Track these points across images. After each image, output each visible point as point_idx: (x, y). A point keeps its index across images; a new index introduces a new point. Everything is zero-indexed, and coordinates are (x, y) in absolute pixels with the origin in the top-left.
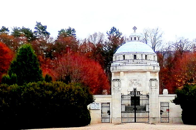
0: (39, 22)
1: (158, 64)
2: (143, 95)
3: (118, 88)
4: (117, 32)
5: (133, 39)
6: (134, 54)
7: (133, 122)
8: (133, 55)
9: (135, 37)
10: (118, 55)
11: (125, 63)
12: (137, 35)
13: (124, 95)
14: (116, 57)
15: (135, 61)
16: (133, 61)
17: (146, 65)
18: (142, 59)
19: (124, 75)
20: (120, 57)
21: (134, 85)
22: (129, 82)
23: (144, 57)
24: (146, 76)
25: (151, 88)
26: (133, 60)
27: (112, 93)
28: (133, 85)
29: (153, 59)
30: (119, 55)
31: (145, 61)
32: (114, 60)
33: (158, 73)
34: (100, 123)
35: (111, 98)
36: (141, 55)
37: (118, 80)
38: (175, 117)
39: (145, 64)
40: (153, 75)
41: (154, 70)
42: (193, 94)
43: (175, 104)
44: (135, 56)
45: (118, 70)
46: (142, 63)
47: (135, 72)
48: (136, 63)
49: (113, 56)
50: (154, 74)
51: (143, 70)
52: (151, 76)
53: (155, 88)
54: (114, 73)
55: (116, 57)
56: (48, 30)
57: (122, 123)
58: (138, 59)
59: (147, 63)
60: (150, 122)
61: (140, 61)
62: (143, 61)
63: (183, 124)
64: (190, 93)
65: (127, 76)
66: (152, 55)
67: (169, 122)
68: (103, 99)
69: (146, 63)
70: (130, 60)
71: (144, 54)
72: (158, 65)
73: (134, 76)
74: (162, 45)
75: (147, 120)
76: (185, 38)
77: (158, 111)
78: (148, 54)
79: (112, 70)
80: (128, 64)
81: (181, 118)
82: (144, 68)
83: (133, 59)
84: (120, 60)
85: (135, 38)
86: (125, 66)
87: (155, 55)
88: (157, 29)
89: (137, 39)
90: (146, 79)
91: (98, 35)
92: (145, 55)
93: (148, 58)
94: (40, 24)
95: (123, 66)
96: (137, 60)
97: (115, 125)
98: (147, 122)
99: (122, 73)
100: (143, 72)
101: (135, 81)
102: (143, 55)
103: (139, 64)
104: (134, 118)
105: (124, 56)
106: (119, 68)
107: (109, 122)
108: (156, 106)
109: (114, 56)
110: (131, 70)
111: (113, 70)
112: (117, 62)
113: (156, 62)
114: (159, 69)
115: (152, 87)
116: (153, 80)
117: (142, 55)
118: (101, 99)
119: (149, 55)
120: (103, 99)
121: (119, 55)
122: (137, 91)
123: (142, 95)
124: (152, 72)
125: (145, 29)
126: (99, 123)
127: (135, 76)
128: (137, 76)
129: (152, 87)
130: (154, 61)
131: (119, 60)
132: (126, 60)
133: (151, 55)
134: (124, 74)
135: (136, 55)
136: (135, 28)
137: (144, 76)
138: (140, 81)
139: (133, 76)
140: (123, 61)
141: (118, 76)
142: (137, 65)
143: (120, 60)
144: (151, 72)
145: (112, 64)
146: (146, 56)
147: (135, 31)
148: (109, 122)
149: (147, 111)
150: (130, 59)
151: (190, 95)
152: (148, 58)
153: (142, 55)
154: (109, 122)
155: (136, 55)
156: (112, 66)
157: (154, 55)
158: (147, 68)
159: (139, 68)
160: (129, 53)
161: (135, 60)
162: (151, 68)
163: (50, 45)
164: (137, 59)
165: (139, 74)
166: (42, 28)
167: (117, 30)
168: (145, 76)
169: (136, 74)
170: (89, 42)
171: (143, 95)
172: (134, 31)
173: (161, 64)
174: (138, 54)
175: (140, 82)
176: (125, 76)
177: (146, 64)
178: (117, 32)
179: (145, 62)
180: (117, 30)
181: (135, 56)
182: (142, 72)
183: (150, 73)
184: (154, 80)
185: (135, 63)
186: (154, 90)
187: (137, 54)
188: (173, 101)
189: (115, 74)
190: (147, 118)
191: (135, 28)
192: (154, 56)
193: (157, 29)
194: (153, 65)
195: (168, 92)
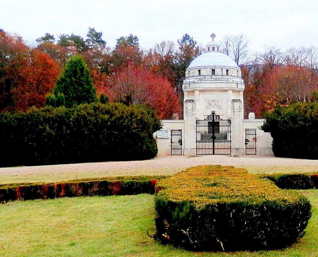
0: (92, 28)
1: (243, 81)
2: (223, 120)
3: (192, 111)
4: (191, 40)
5: (211, 49)
6: (212, 68)
7: (211, 154)
8: (211, 69)
9: (213, 46)
10: (192, 70)
11: (201, 79)
12: (216, 44)
13: (200, 120)
14: (189, 72)
15: (213, 77)
16: (211, 77)
17: (227, 83)
18: (222, 75)
19: (200, 95)
20: (194, 72)
21: (213, 107)
22: (206, 104)
23: (225, 72)
24: (227, 96)
25: (234, 112)
26: (211, 75)
27: (185, 118)
28: (211, 107)
29: (236, 75)
30: (193, 70)
31: (226, 77)
32: (187, 75)
33: (242, 92)
34: (170, 155)
35: (184, 123)
36: (221, 69)
37: (191, 101)
38: (264, 148)
40: (236, 94)
41: (237, 88)
42: (286, 119)
43: (264, 131)
44: (213, 71)
45: (192, 89)
46: (222, 80)
47: (214, 90)
48: (215, 79)
49: (185, 71)
50: (237, 94)
52: (233, 96)
53: (239, 111)
54: (187, 92)
55: (189, 72)
56: (103, 38)
57: (197, 155)
58: (218, 74)
59: (228, 80)
60: (233, 154)
63: (273, 157)
64: (283, 118)
65: (203, 96)
66: (234, 69)
67: (256, 154)
68: (172, 125)
69: (227, 79)
70: (207, 76)
71: (225, 68)
72: (243, 82)
73: (212, 96)
74: (247, 56)
75: (228, 152)
76: (277, 48)
77: (243, 140)
78: (230, 68)
79: (185, 89)
80: (205, 80)
81: (271, 149)
82: (224, 86)
83: (211, 74)
84: (194, 76)
85: (213, 47)
87: (239, 70)
88: (241, 37)
89: (216, 49)
90: (227, 99)
91: (167, 44)
94: (93, 30)
95: (198, 83)
96: (216, 75)
97: (188, 157)
98: (229, 154)
99: (197, 92)
100: (224, 91)
101: (213, 103)
102: (223, 69)
103: (219, 80)
104: (212, 150)
105: (199, 71)
106: (193, 86)
107: (181, 154)
108: (240, 134)
109: (188, 70)
110: (208, 89)
111: (186, 88)
112: (191, 78)
113: (240, 79)
114: (243, 87)
115: (235, 110)
116: (236, 101)
117: (222, 69)
118: (171, 125)
119: (231, 69)
120: (172, 125)
121: (193, 69)
122: (216, 115)
123: (222, 119)
124: (235, 91)
125: (226, 36)
126: (168, 155)
127: (214, 96)
129: (235, 110)
130: (237, 77)
131: (193, 76)
132: (202, 76)
133: (234, 69)
134: (200, 93)
135: (215, 69)
136: (213, 36)
137: (224, 96)
138: (219, 102)
139: (211, 96)
140: (198, 78)
141: (193, 96)
142: (216, 83)
143: (194, 76)
144: (234, 91)
145: (184, 81)
146: (227, 71)
147: (213, 39)
148: (180, 155)
149: (228, 140)
150: (207, 75)
151: (283, 120)
152: (229, 74)
153: (222, 69)
154: (180, 155)
155: (215, 69)
156: (184, 83)
157: (237, 69)
158: (229, 85)
159: (218, 85)
160: (205, 67)
161: (213, 76)
162: (234, 86)
163: (107, 57)
164: (215, 74)
165: (218, 93)
166: (97, 35)
167: (191, 38)
168: (226, 96)
169: (215, 93)
170: (156, 53)
171: (223, 120)
172: (212, 38)
173: (247, 81)
174: (217, 69)
175: (219, 104)
176: (200, 96)
177: (227, 81)
178: (191, 40)
179: (226, 78)
180: (191, 38)
181: (213, 71)
182: (223, 90)
183: (232, 92)
184: (237, 101)
185: (213, 80)
186: (237, 113)
187: (216, 68)
188: (261, 128)
189: (188, 93)
190: (229, 149)
191: (213, 36)
192: (238, 71)
193: (241, 37)
195: (255, 117)
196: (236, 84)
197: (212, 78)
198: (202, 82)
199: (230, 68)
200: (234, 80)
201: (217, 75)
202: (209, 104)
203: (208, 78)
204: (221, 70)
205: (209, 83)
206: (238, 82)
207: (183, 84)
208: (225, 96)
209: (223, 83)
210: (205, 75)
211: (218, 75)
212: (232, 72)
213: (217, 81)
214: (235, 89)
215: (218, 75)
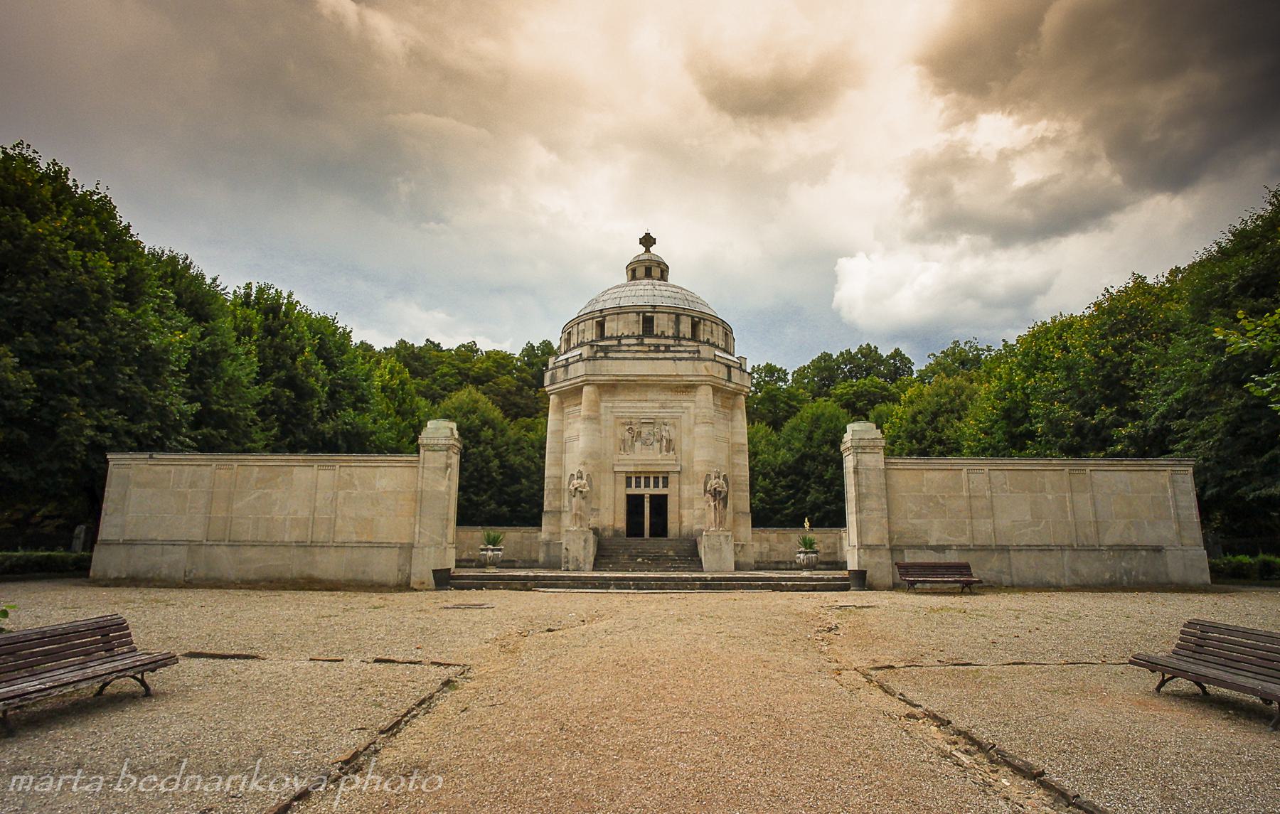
10: (578, 324)
15: (647, 341)
17: (699, 359)
18: (676, 335)
21: (644, 443)
22: (623, 432)
23: (686, 328)
26: (639, 335)
28: (638, 445)
39: (691, 355)
45: (572, 382)
46: (679, 352)
47: (648, 386)
48: (652, 348)
51: (684, 378)
58: (663, 332)
59: (698, 352)
61: (671, 342)
62: (684, 342)
69: (696, 349)
71: (688, 316)
73: (644, 404)
80: (620, 351)
82: (685, 369)
86: (606, 362)
89: (656, 272)
93: (702, 336)
102: (683, 318)
105: (601, 325)
117: (678, 316)
128: (657, 405)
132: (611, 338)
134: (600, 395)
136: (648, 241)
138: (667, 428)
142: (658, 359)
146: (695, 326)
150: (626, 334)
153: (678, 316)
156: (550, 367)
159: (665, 368)
160: (620, 311)
161: (647, 337)
164: (655, 333)
181: (648, 323)
182: (678, 387)
185: (647, 349)
191: (648, 241)
194: (726, 361)
196: (725, 370)
197: (642, 344)
198: (610, 355)
200: (717, 353)
201: (659, 334)
202: (634, 433)
203: (629, 345)
204: (674, 319)
205: (634, 359)
206: (731, 364)
207: (547, 368)
208: (687, 408)
209: (680, 359)
210: (619, 335)
211: (663, 336)
213: (661, 355)
214: (724, 383)
215: (663, 336)
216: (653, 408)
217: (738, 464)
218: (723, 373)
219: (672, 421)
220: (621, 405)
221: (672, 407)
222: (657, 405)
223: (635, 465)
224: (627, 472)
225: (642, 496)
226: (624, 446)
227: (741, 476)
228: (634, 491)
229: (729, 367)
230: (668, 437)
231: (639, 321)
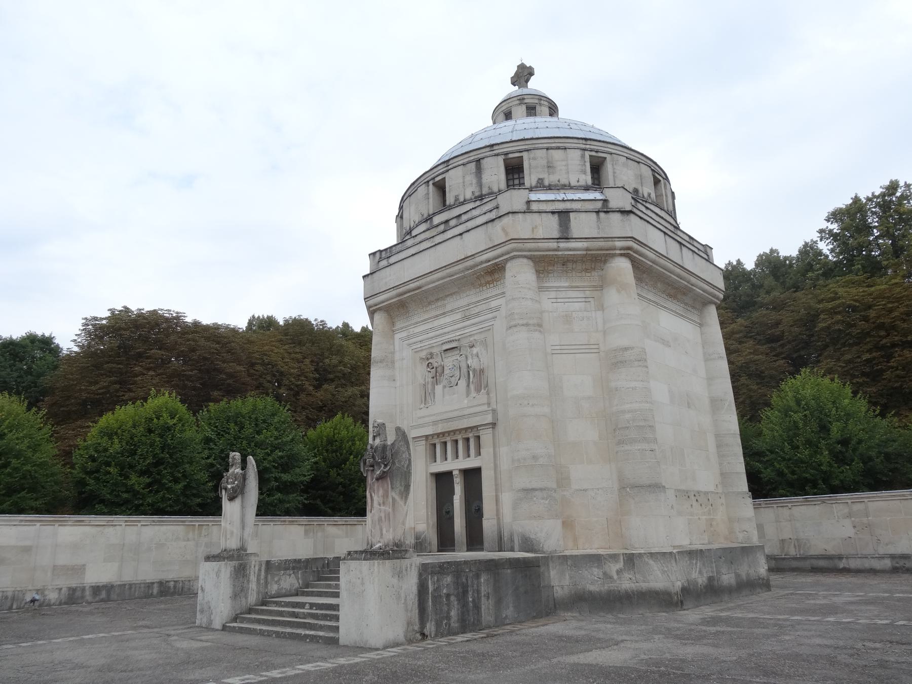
36: (473, 165)
58: (457, 199)
65: (404, 334)
92: (501, 159)
100: (489, 278)
101: (449, 361)
110: (412, 286)
117: (478, 161)
119: (541, 153)
127: (447, 319)
128: (458, 316)
136: (523, 75)
137: (494, 304)
138: (475, 350)
139: (436, 323)
196: (555, 219)
199: (528, 150)
208: (497, 309)
212: (544, 162)
214: (553, 245)
216: (455, 322)
217: (616, 389)
218: (549, 226)
219: (482, 336)
220: (417, 330)
221: (478, 315)
222: (458, 316)
223: (435, 423)
224: (427, 437)
225: (449, 474)
226: (427, 396)
227: (623, 412)
228: (441, 467)
229: (564, 215)
230: (477, 368)
231: (428, 194)
